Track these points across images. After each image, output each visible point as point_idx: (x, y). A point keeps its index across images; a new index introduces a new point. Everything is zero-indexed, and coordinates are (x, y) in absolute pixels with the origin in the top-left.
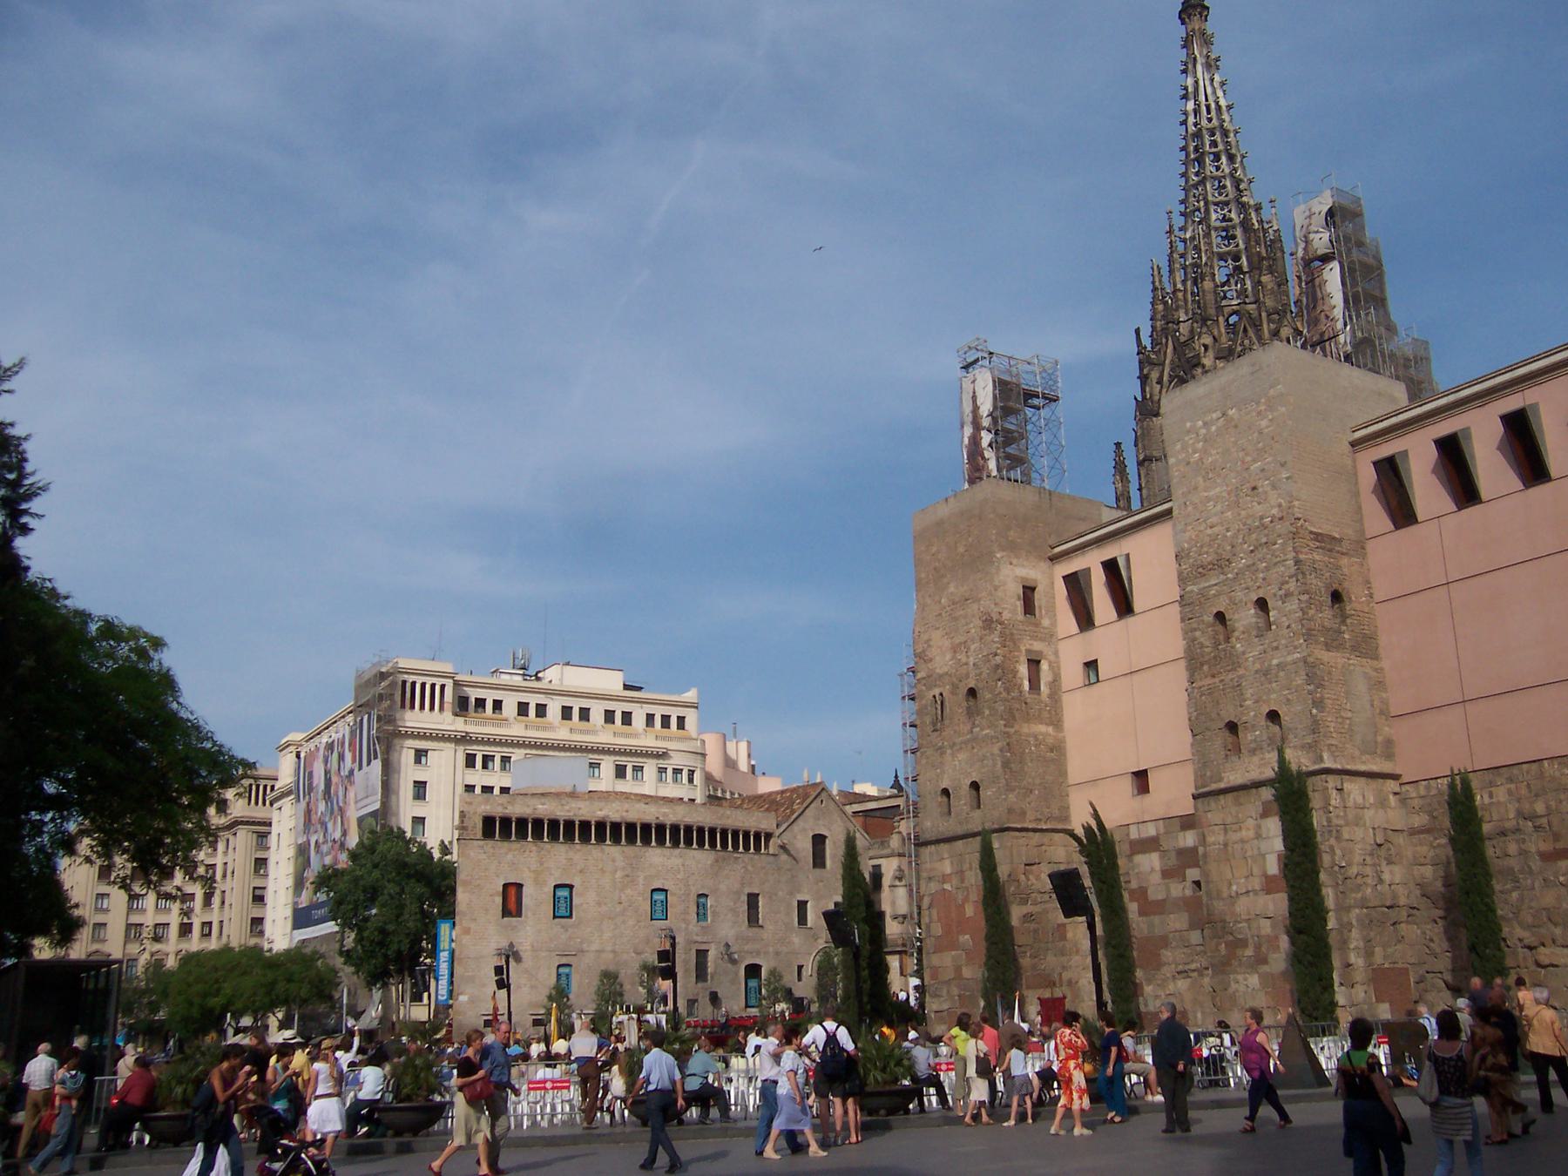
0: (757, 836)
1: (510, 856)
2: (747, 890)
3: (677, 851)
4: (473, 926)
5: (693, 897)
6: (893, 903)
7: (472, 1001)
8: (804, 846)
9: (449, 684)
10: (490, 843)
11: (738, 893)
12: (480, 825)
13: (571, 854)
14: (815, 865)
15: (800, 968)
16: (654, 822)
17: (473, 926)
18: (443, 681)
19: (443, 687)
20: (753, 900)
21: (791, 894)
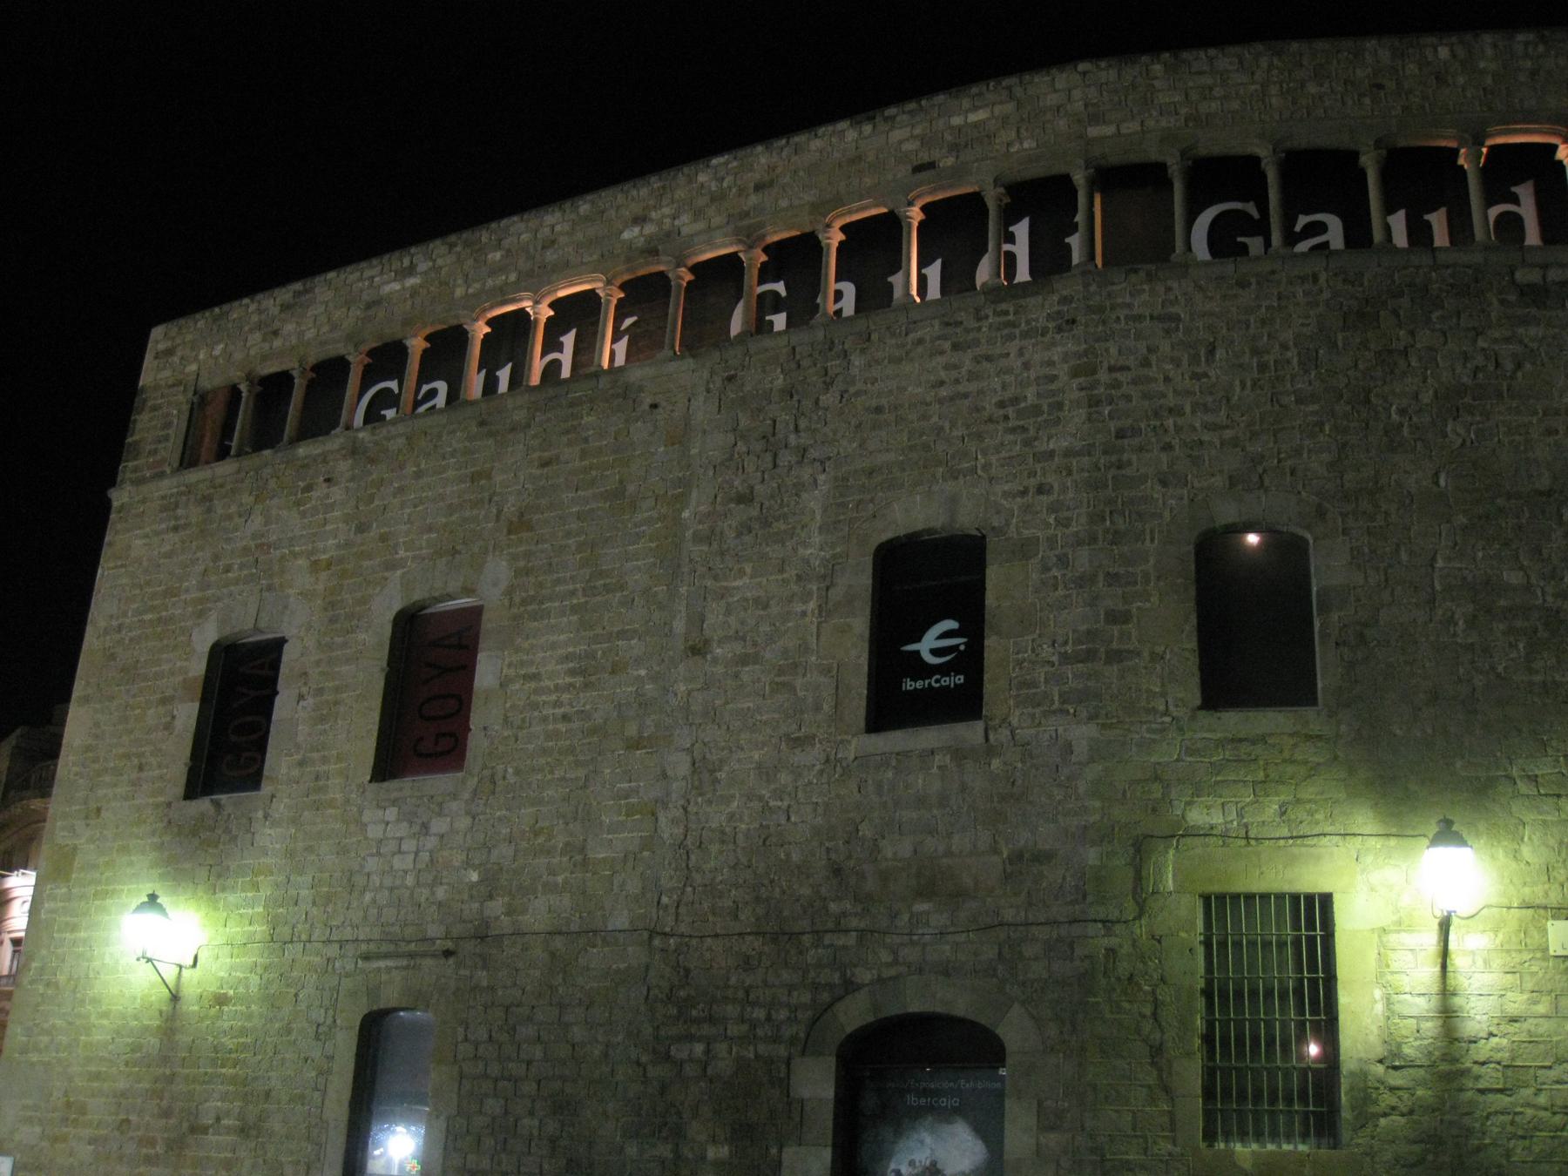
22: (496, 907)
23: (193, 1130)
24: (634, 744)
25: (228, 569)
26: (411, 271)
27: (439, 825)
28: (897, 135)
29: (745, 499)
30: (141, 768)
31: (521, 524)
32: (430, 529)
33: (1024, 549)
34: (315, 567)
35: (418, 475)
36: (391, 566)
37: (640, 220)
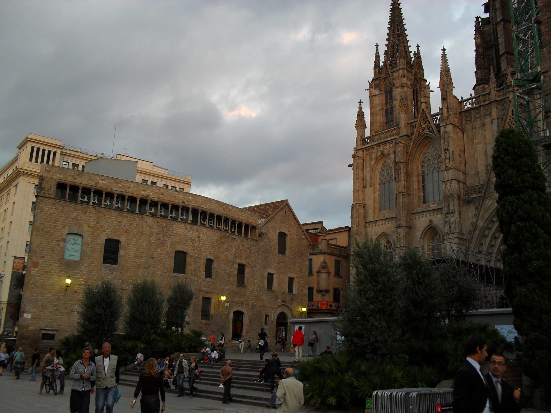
0: (247, 226)
1: (75, 214)
2: (238, 261)
3: (195, 227)
4: (40, 261)
5: (203, 261)
6: (318, 283)
7: (34, 318)
8: (274, 237)
9: (59, 152)
10: (61, 203)
11: (233, 262)
12: (54, 188)
13: (120, 219)
14: (279, 252)
15: (267, 316)
16: (181, 205)
17: (40, 261)
18: (55, 150)
19: (55, 153)
20: (241, 268)
21: (264, 268)
22: (124, 286)
23: (72, 311)
24: (144, 268)
25: (69, 221)
26: (104, 180)
27: (114, 273)
28: (180, 196)
29: (160, 239)
30: (53, 251)
31: (126, 232)
32: (111, 227)
33: (191, 257)
34: (89, 227)
35: (108, 218)
36: (103, 231)
37: (144, 191)
